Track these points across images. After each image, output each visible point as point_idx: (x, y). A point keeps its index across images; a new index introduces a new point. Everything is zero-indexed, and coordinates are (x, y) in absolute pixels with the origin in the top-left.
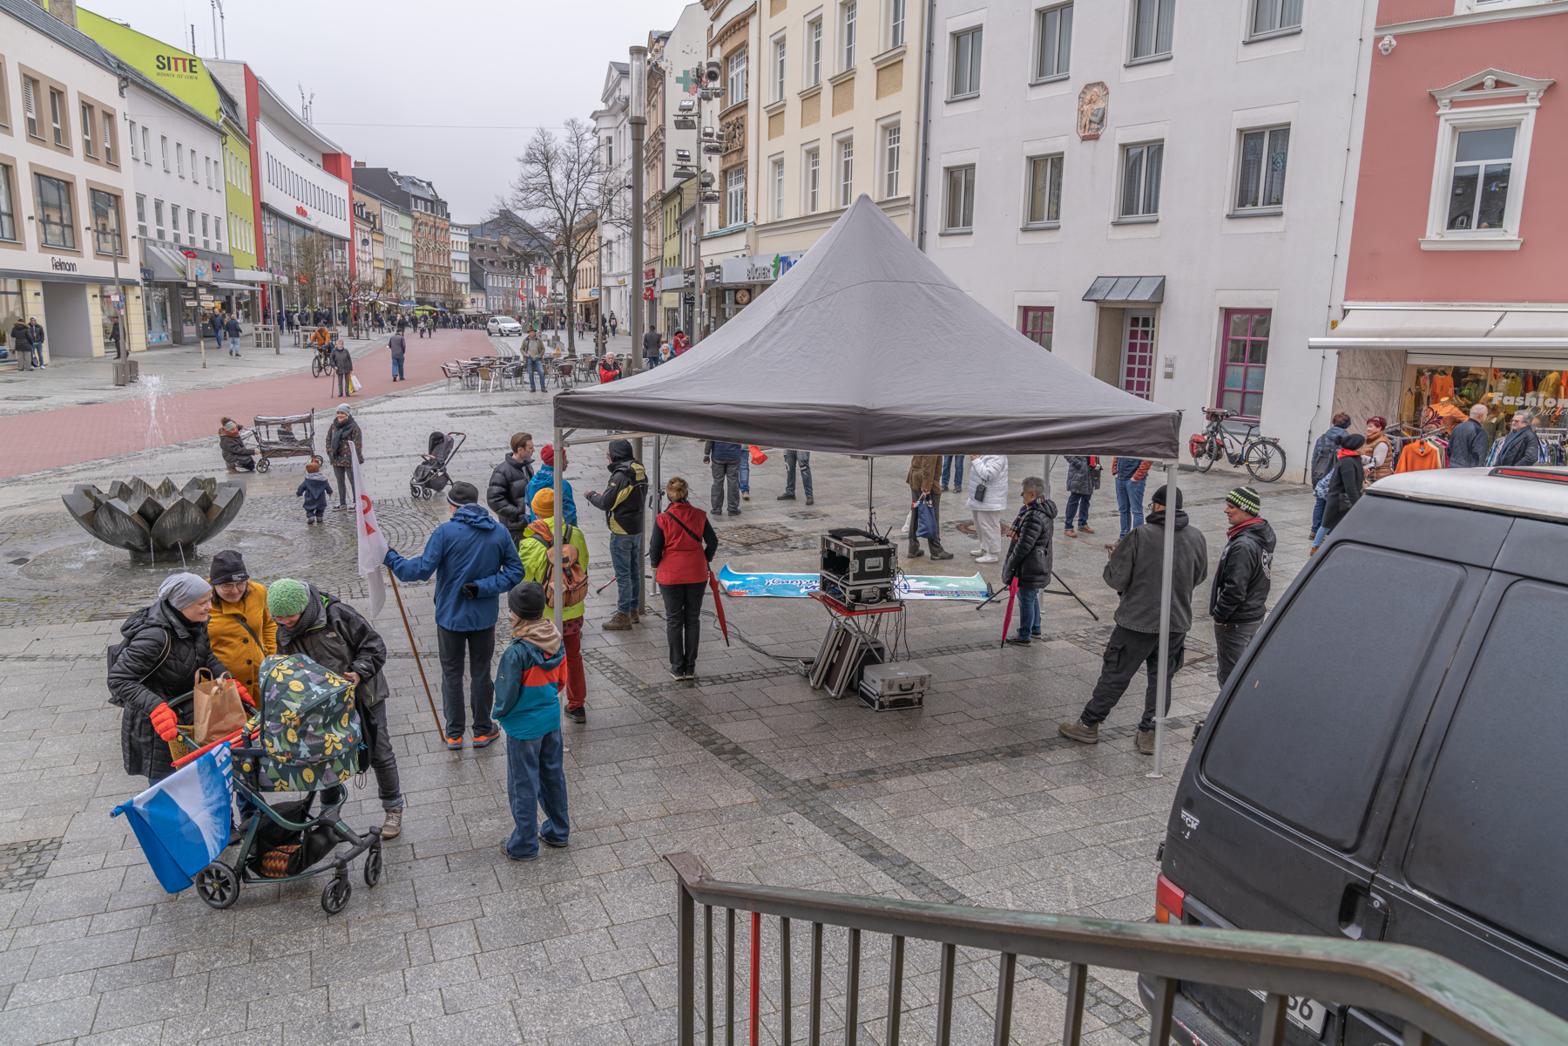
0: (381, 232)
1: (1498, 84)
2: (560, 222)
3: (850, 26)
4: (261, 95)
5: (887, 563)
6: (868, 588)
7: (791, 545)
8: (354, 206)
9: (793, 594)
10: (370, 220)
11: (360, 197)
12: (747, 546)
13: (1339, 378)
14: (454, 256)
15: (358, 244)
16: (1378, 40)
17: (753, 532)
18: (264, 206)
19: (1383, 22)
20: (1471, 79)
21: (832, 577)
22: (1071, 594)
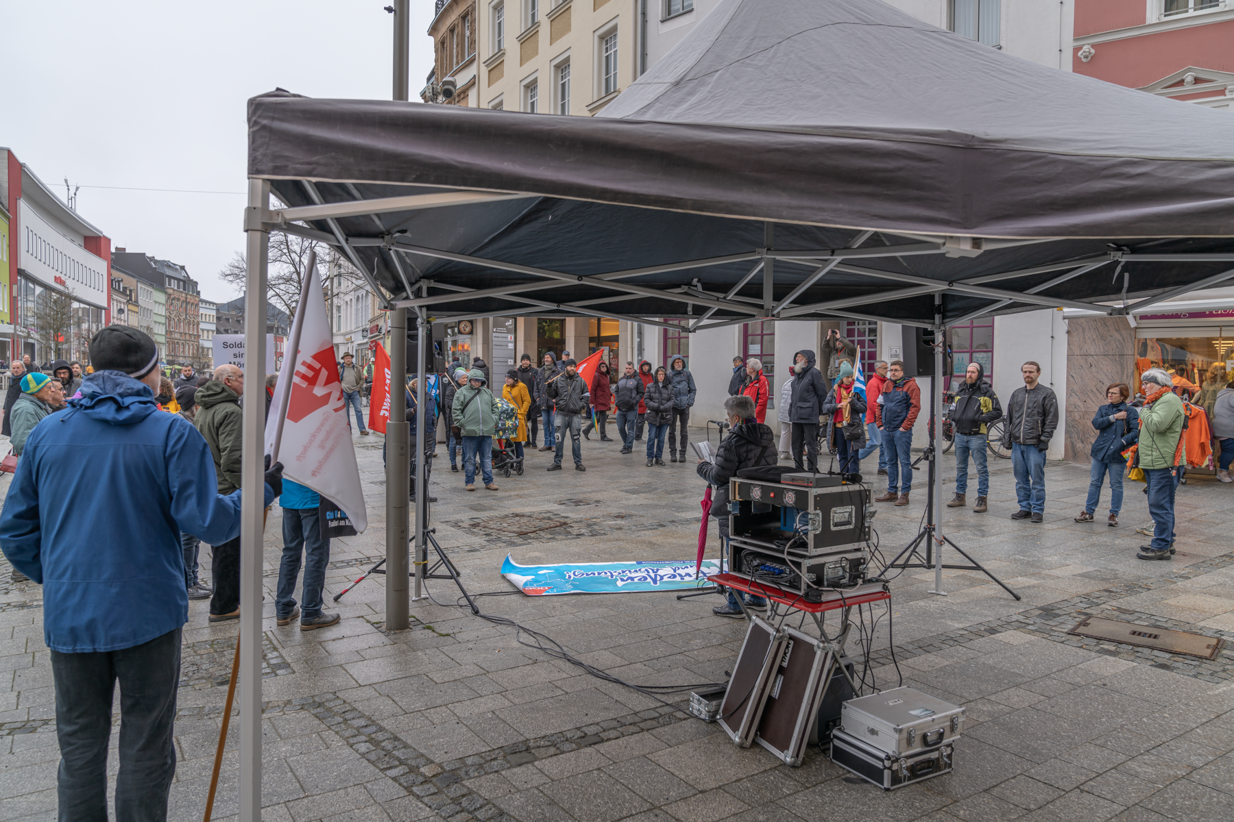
0: (136, 304)
1: (1197, 81)
2: (295, 276)
3: (563, 85)
4: (24, 180)
5: (862, 517)
6: (832, 560)
7: (575, 532)
8: (111, 282)
9: (610, 589)
10: (128, 294)
11: (116, 274)
12: (522, 534)
13: (1070, 356)
14: (202, 326)
15: (114, 312)
16: (1077, 50)
17: (524, 520)
18: (21, 272)
19: (1079, 34)
20: (1172, 77)
21: (750, 544)
22: (978, 568)
